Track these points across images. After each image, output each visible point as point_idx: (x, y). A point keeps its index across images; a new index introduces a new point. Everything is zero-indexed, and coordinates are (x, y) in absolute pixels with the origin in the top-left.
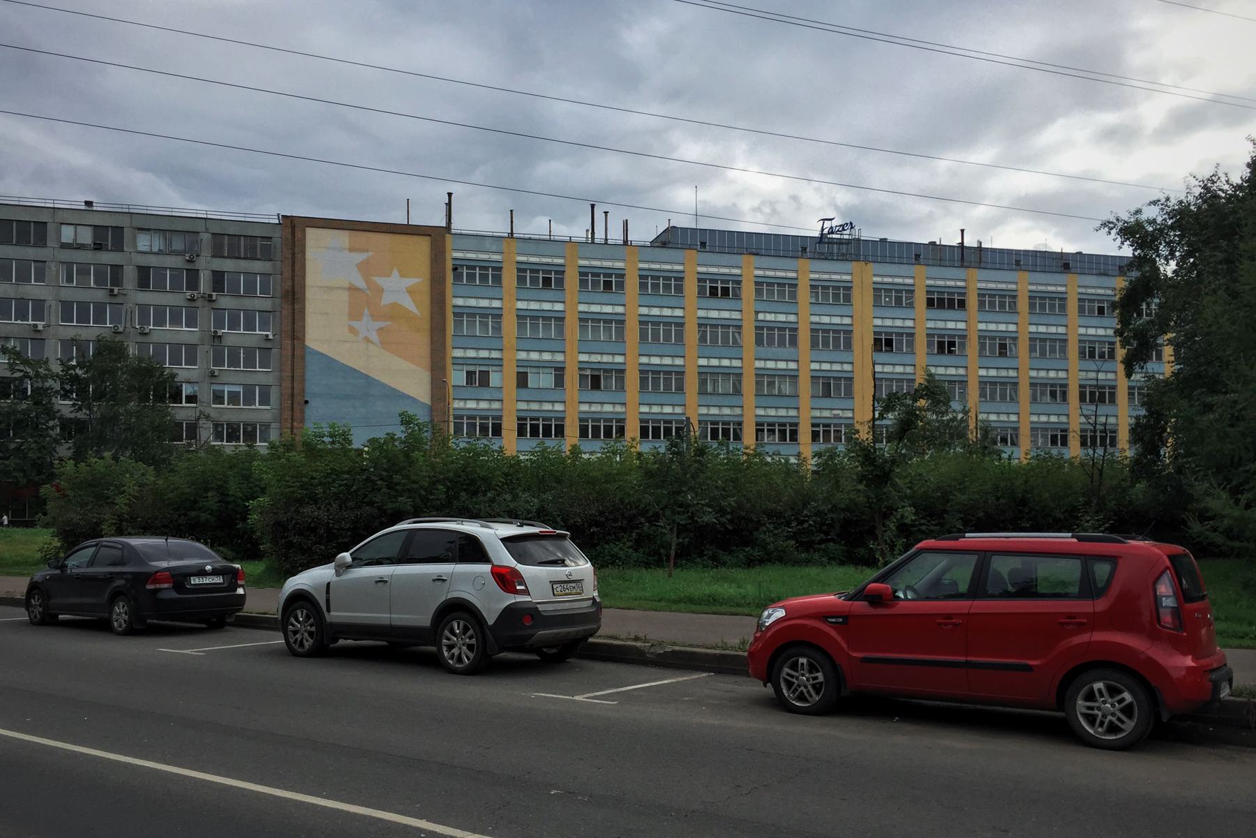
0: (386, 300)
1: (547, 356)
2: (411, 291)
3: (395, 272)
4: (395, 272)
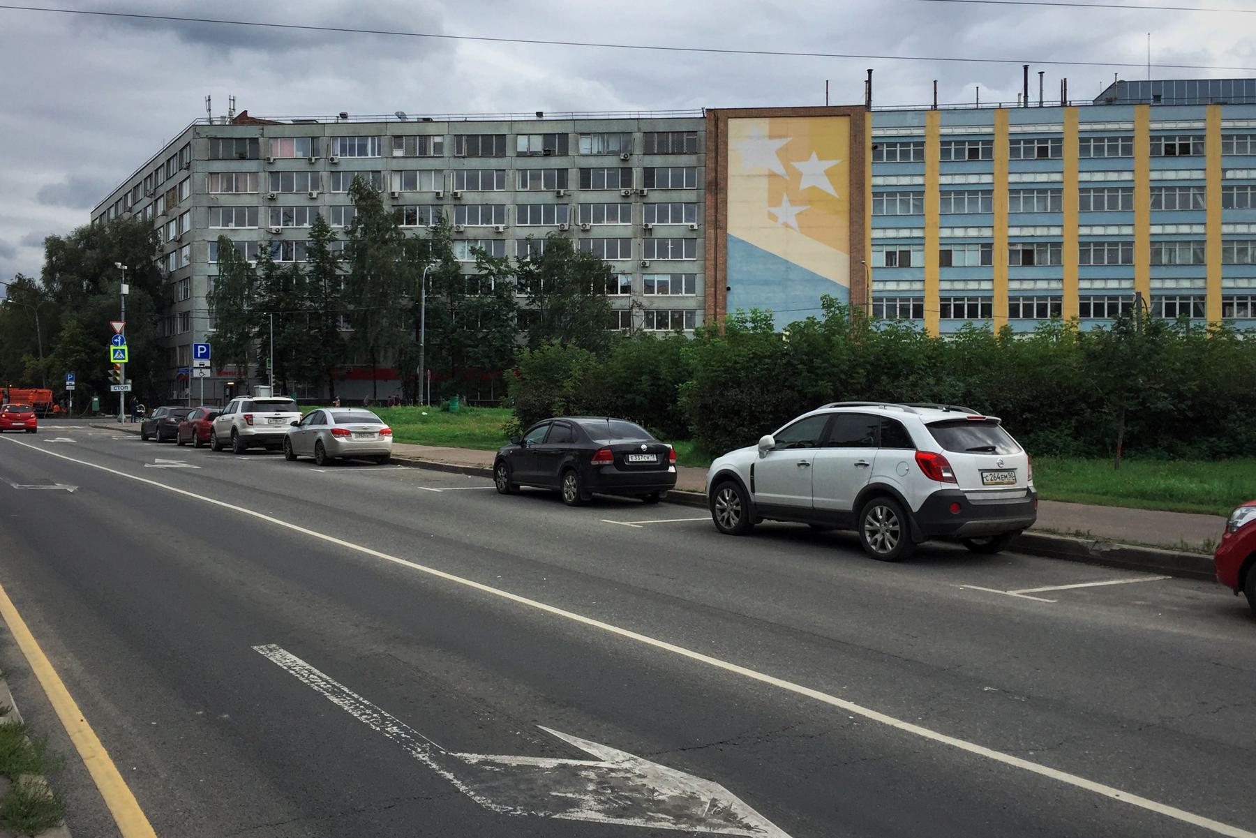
0: (805, 184)
1: (973, 233)
2: (829, 174)
4: (814, 155)
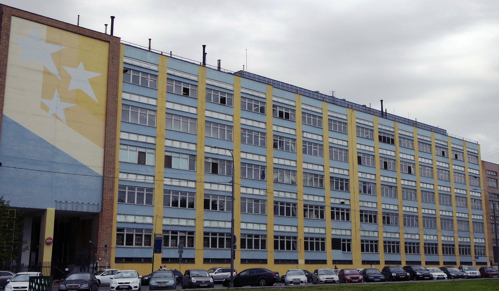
0: (73, 86)
1: (184, 146)
2: (92, 82)
3: (81, 65)
4: (81, 65)
